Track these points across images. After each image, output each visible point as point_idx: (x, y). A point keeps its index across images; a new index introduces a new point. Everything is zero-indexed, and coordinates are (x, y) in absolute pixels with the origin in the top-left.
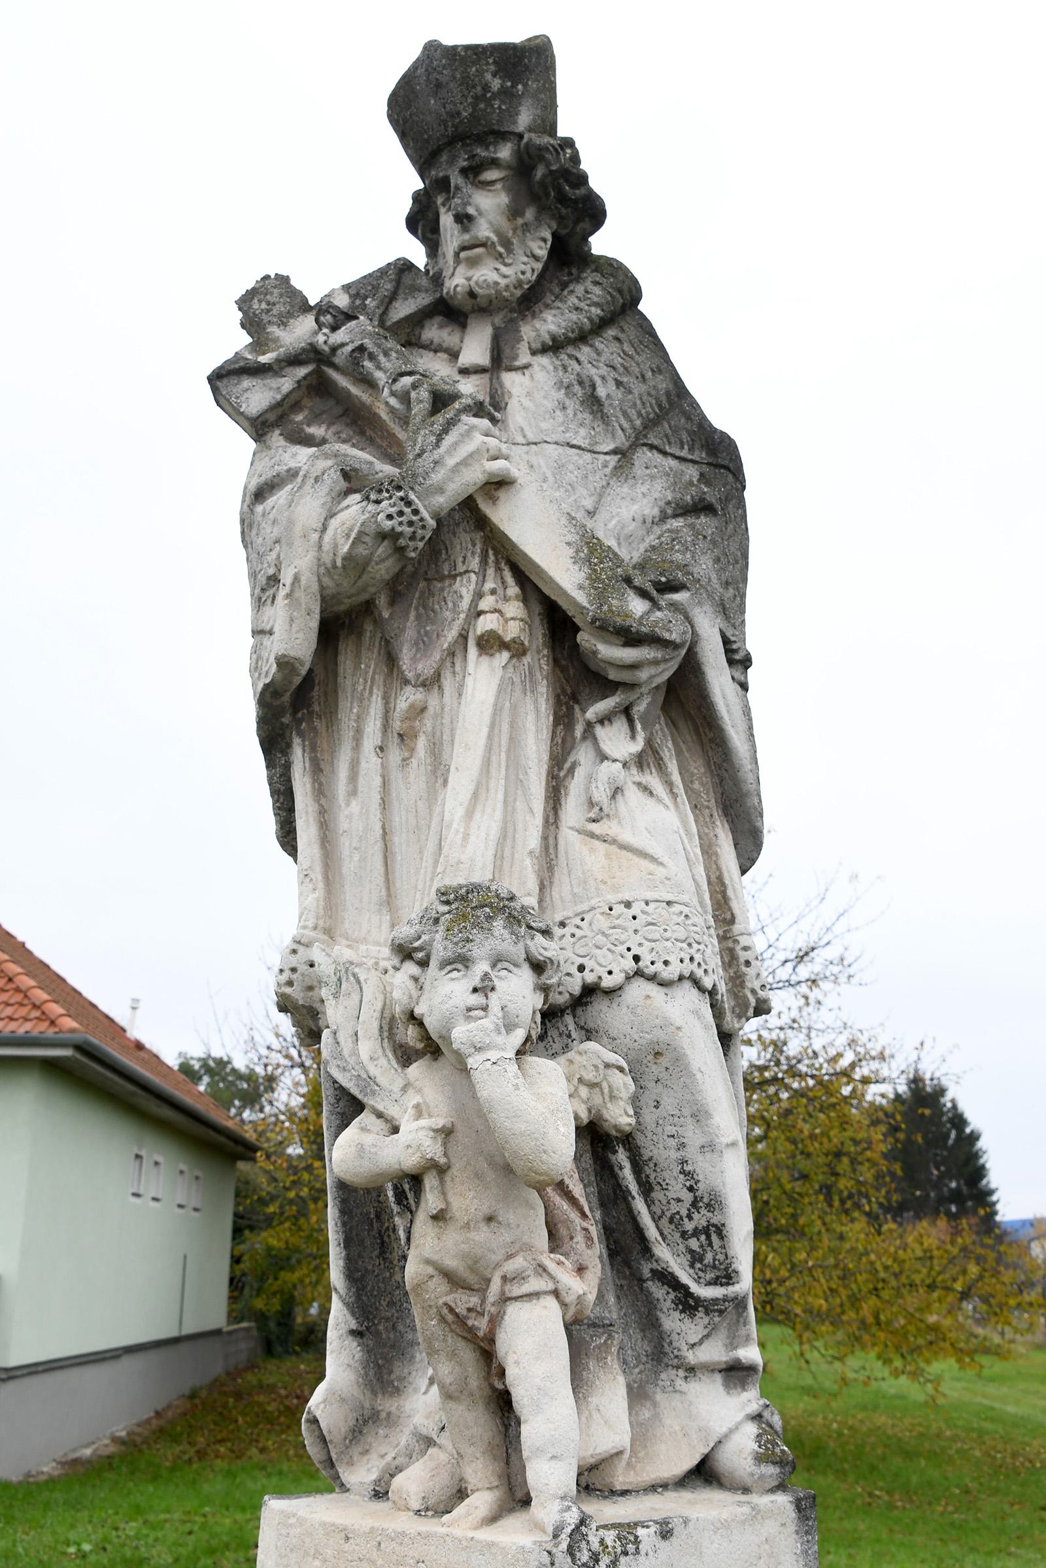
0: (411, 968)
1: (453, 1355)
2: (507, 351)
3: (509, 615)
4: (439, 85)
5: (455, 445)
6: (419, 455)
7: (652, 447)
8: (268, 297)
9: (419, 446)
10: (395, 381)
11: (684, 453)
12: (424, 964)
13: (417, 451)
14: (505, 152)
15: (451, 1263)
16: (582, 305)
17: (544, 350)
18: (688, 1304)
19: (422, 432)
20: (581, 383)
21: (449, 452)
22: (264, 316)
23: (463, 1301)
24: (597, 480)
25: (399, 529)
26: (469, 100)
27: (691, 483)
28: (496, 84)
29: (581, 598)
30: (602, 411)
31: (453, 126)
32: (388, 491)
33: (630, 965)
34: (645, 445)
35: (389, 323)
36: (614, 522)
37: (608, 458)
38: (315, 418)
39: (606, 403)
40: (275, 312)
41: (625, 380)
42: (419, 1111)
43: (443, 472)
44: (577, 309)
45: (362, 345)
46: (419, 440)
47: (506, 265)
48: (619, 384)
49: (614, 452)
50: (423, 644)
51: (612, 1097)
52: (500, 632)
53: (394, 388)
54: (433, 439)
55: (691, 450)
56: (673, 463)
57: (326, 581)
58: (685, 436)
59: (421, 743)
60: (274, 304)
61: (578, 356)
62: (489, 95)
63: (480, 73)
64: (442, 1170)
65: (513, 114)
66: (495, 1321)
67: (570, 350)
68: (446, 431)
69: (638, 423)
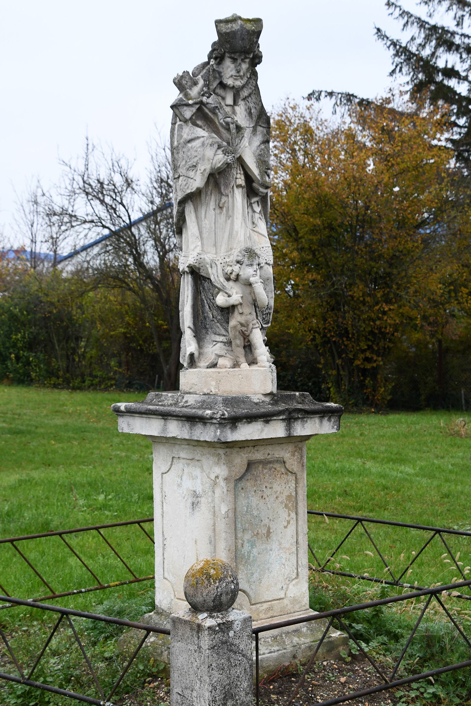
0: (239, 265)
1: (240, 339)
4: (243, 39)
12: (241, 264)
15: (243, 322)
23: (244, 329)
29: (259, 177)
38: (197, 118)
42: (237, 293)
50: (227, 186)
56: (262, 128)
59: (224, 209)
64: (241, 304)
66: (251, 332)
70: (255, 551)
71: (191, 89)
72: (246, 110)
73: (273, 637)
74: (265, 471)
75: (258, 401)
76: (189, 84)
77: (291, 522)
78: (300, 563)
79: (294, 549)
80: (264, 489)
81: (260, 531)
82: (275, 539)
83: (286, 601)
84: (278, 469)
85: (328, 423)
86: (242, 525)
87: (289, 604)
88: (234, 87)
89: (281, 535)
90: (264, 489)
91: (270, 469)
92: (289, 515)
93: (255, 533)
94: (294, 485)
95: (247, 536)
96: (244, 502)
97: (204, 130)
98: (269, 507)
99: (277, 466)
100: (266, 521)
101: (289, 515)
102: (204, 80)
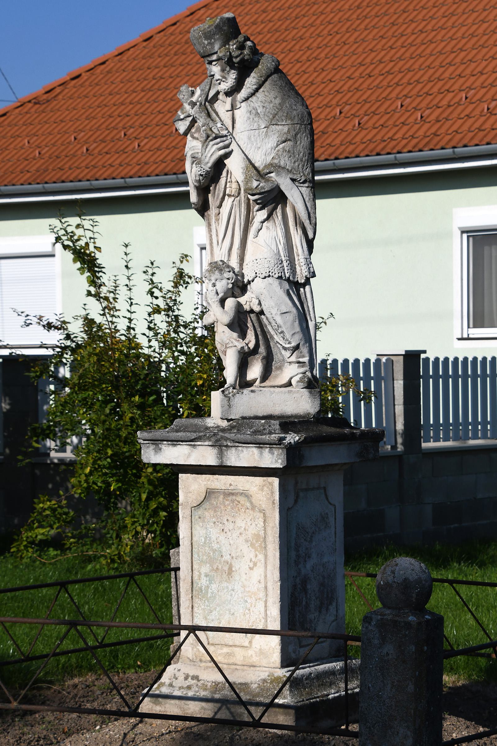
2: (234, 105)
5: (209, 151)
7: (273, 125)
14: (215, 57)
17: (243, 101)
18: (285, 349)
27: (285, 133)
33: (254, 275)
35: (209, 99)
41: (265, 105)
48: (264, 107)
49: (265, 128)
51: (254, 305)
55: (286, 121)
56: (280, 127)
57: (196, 184)
58: (283, 118)
63: (202, 40)
65: (213, 48)
67: (250, 99)
68: (206, 148)
69: (271, 117)
70: (214, 587)
73: (215, 682)
74: (227, 503)
75: (212, 425)
76: (186, 97)
77: (258, 564)
78: (268, 612)
79: (262, 595)
80: (226, 522)
81: (220, 567)
82: (237, 578)
83: (250, 652)
84: (242, 502)
85: (271, 456)
86: (199, 556)
87: (254, 655)
89: (244, 577)
90: (226, 522)
91: (233, 501)
92: (256, 556)
93: (215, 568)
94: (262, 524)
95: (205, 569)
96: (202, 532)
98: (232, 542)
99: (242, 499)
100: (227, 558)
101: (256, 556)
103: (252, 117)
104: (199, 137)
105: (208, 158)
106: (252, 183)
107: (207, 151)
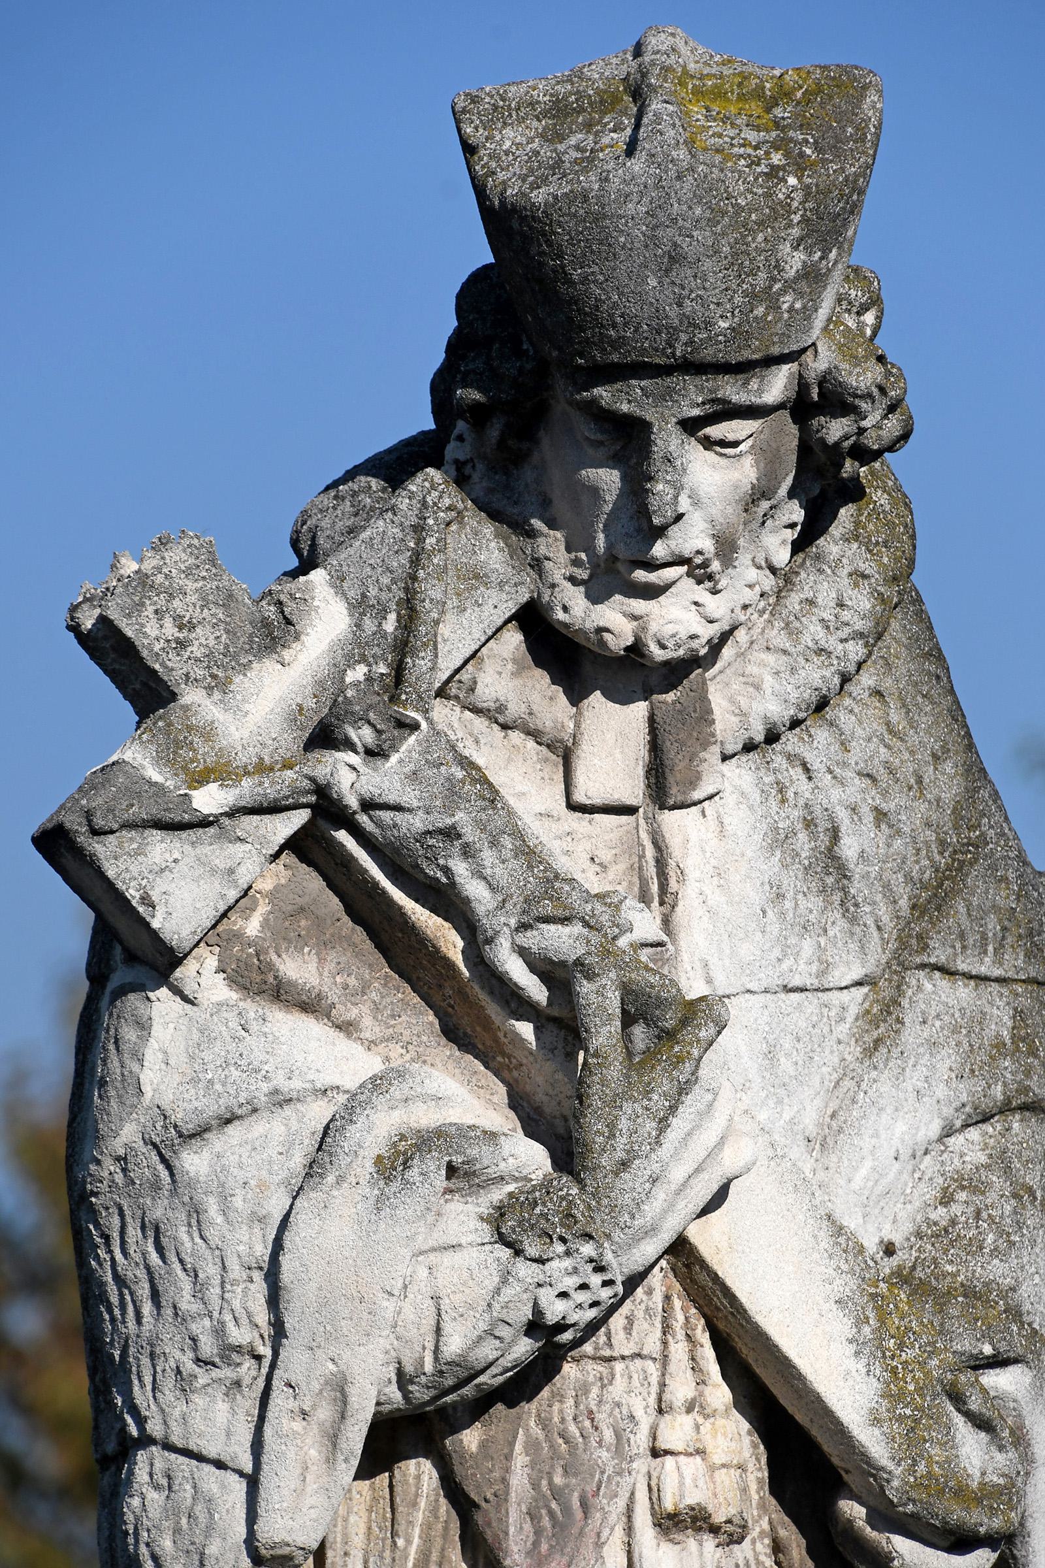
3: (718, 1458)
4: (675, 258)
6: (624, 1165)
8: (176, 603)
9: (621, 1141)
10: (523, 927)
11: (986, 967)
13: (620, 1155)
16: (832, 643)
17: (749, 747)
19: (628, 1107)
20: (809, 824)
21: (676, 1155)
22: (173, 660)
24: (829, 1060)
25: (573, 1318)
26: (738, 299)
28: (795, 261)
30: (845, 890)
31: (691, 342)
32: (563, 1240)
34: (923, 966)
36: (863, 1172)
37: (845, 996)
39: (857, 871)
40: (196, 650)
43: (661, 1196)
44: (820, 651)
45: (453, 827)
46: (624, 1124)
47: (715, 592)
48: (880, 816)
49: (859, 984)
52: (710, 1509)
53: (521, 939)
54: (650, 1126)
56: (964, 992)
58: (992, 924)
60: (192, 627)
61: (809, 757)
62: (777, 286)
67: (791, 742)
68: (673, 1109)
71: (219, 685)
72: (779, 840)
76: (204, 639)
88: (636, 649)
97: (347, 1028)
102: (359, 606)
103: (791, 881)
104: (333, 995)
105: (660, 1195)
106: (949, 1442)
107: (672, 1136)
